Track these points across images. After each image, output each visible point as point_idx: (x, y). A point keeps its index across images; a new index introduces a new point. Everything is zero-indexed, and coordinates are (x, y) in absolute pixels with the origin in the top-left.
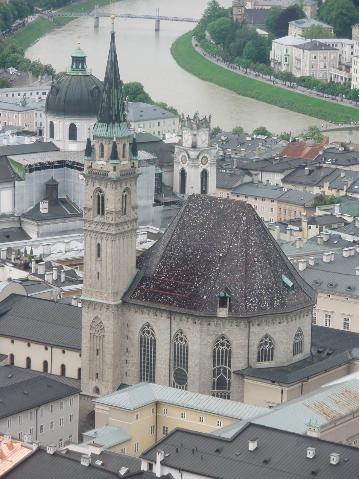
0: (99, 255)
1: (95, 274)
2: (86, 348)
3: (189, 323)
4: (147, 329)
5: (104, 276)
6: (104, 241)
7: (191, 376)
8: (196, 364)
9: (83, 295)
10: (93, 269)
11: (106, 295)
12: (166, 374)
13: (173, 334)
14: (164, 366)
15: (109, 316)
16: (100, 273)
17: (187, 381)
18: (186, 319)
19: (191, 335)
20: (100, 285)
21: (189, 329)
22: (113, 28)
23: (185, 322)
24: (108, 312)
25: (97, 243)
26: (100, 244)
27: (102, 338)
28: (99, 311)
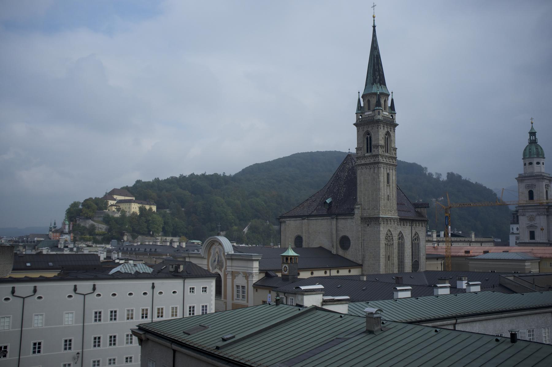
0: (388, 182)
1: (386, 197)
2: (383, 257)
3: (420, 227)
4: (401, 237)
5: (391, 197)
6: (391, 171)
9: (380, 214)
10: (385, 193)
11: (393, 212)
13: (413, 237)
14: (409, 261)
15: (396, 227)
16: (389, 195)
17: (418, 268)
18: (418, 225)
19: (421, 235)
20: (389, 205)
21: (420, 231)
23: (418, 226)
24: (395, 224)
27: (392, 246)
28: (390, 225)
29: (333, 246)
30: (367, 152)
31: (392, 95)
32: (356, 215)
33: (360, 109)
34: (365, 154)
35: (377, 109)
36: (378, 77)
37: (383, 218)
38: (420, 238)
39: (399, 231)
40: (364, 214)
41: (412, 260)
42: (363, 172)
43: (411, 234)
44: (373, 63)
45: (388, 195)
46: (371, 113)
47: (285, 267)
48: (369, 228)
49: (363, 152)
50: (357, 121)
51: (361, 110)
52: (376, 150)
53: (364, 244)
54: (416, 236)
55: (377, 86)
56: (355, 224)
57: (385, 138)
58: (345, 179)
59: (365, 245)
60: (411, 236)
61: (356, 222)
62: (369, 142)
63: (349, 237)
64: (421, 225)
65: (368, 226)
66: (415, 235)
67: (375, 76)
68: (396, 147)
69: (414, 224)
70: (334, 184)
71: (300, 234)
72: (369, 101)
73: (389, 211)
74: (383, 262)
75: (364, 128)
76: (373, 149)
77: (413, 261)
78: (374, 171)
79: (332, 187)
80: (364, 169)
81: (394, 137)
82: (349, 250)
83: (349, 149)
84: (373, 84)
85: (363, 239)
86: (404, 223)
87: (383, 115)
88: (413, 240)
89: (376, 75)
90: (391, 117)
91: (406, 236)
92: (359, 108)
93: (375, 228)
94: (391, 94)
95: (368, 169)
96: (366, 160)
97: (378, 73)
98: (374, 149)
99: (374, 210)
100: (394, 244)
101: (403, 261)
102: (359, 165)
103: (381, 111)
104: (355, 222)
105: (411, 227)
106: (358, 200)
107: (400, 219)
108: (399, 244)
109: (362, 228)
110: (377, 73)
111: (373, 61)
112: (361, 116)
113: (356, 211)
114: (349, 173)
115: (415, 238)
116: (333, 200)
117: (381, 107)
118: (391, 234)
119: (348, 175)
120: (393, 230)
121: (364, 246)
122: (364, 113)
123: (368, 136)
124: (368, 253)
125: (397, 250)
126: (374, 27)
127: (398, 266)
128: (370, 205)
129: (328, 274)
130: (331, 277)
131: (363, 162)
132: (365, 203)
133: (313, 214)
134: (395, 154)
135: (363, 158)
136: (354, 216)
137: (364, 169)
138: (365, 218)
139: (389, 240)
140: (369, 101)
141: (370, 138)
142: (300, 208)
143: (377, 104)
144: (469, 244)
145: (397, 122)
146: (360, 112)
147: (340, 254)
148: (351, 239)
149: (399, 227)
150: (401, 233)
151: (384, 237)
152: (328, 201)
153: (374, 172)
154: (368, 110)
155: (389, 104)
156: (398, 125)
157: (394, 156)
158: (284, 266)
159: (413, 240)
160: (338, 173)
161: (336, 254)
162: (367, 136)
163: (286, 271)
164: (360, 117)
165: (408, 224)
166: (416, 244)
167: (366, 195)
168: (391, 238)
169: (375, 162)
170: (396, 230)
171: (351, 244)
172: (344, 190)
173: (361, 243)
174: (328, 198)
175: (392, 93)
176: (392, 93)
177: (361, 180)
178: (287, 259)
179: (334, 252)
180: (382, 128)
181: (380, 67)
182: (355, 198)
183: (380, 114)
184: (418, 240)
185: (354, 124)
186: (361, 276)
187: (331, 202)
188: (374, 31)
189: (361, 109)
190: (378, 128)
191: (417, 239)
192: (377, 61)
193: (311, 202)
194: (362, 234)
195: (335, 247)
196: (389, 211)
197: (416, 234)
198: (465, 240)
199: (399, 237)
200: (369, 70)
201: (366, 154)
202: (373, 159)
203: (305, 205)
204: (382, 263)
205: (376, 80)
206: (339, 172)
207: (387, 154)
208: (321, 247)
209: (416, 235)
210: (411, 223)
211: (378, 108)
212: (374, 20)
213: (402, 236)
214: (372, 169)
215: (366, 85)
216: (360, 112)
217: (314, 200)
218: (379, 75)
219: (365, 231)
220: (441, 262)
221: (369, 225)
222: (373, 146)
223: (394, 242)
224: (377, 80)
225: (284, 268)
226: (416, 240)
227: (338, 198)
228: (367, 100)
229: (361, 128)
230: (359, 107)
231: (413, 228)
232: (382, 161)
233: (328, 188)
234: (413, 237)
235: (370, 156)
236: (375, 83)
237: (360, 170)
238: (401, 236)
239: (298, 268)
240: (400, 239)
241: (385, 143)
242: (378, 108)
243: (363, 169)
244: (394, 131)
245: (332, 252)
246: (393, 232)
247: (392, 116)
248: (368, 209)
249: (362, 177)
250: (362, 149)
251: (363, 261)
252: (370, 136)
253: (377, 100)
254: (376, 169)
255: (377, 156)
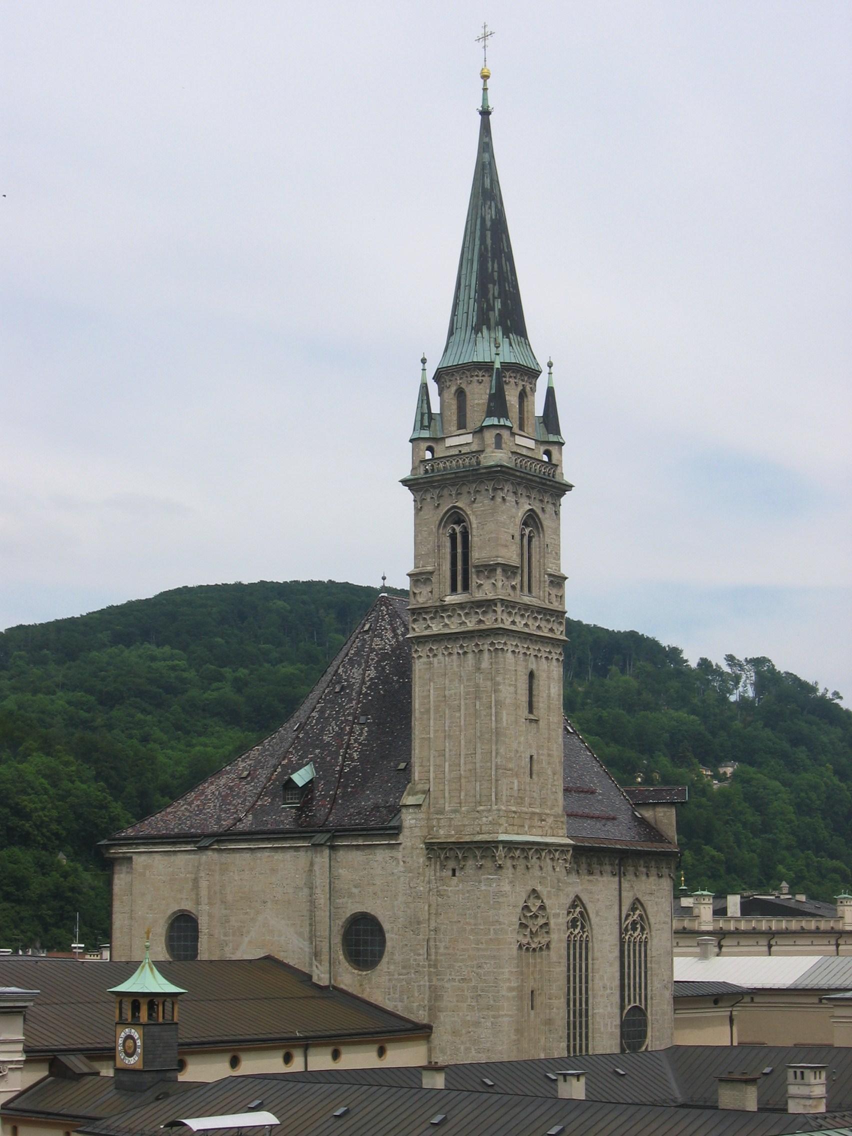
2: (510, 994)
7: (659, 1017)
8: (665, 982)
11: (550, 820)
12: (614, 1030)
13: (624, 916)
14: (609, 1008)
15: (558, 882)
16: (535, 757)
18: (644, 870)
22: (485, 99)
25: (530, 670)
26: (535, 672)
29: (316, 954)
30: (454, 589)
31: (550, 373)
32: (406, 832)
33: (426, 423)
34: (446, 596)
35: (493, 426)
36: (498, 305)
37: (510, 846)
38: (652, 920)
39: (572, 896)
40: (437, 831)
41: (622, 1008)
42: (436, 665)
43: (616, 908)
44: (480, 249)
45: (531, 757)
46: (468, 438)
47: (129, 1037)
48: (457, 886)
49: (436, 590)
50: (414, 469)
51: (429, 427)
52: (487, 585)
53: (436, 947)
54: (638, 912)
55: (493, 335)
56: (402, 869)
57: (522, 536)
58: (366, 694)
59: (442, 950)
60: (617, 913)
61: (407, 860)
62: (459, 550)
63: (381, 919)
64: (654, 871)
65: (454, 875)
66: (633, 909)
67: (488, 301)
68: (564, 571)
69: (631, 869)
70: (322, 712)
71: (187, 906)
72: (461, 394)
73: (536, 818)
74: (511, 1016)
75: (440, 497)
76: (474, 580)
77: (626, 1011)
78: (479, 661)
79: (316, 724)
80: (440, 657)
81: (557, 531)
82: (378, 967)
83: (384, 578)
84: (477, 330)
85: (433, 925)
86: (589, 865)
87: (515, 449)
88: (626, 930)
89: (491, 293)
90: (545, 458)
91: (597, 914)
92: (425, 417)
93: (480, 882)
94: (545, 369)
95: (455, 657)
96: (446, 621)
97: (497, 287)
98: (478, 577)
99: (477, 815)
100: (552, 946)
101: (587, 1010)
102: (421, 640)
103: (505, 434)
104: (404, 862)
105: (617, 879)
106: (416, 776)
107: (575, 848)
108: (570, 942)
109: (429, 882)
110: (494, 290)
111: (477, 242)
112: (430, 449)
113: (408, 819)
114: (384, 668)
115: (634, 923)
116: (317, 772)
117: (507, 418)
118: (542, 908)
119: (376, 677)
120: (549, 892)
121: (436, 953)
122: (439, 440)
123: (458, 529)
124: (454, 980)
125: (566, 969)
126: (485, 113)
127: (569, 1029)
128: (463, 794)
129: (297, 1065)
130: (308, 1077)
131: (436, 628)
132: (441, 787)
133: (240, 827)
134: (561, 598)
135: (436, 612)
136: (401, 837)
137: (440, 657)
138: (443, 846)
139: (534, 930)
140: (461, 394)
141: (465, 535)
142: (190, 804)
143: (492, 404)
144: (833, 942)
145: (568, 478)
146: (426, 434)
147: (342, 986)
148: (386, 926)
149: (574, 878)
150: (577, 901)
151: (515, 920)
152: (301, 777)
153: (479, 669)
154: (459, 428)
155: (539, 408)
156: (569, 487)
157: (555, 606)
158: (123, 1035)
159: (626, 930)
160: (340, 671)
161: (327, 987)
162: (454, 530)
163: (130, 1055)
164: (428, 455)
165: (608, 868)
166: (635, 943)
167: (447, 755)
168: (541, 921)
169: (482, 627)
170: (561, 893)
171: (389, 944)
172: (361, 734)
173: (428, 941)
174: (300, 766)
175: (550, 365)
176: (550, 365)
177: (429, 695)
178: (136, 1007)
179: (321, 976)
180: (511, 498)
181: (506, 267)
182: (402, 766)
183: (503, 445)
184: (643, 929)
185: (405, 482)
186: (424, 1073)
187: (311, 781)
188: (486, 129)
189: (430, 423)
190: (493, 498)
191: (641, 926)
192: (492, 244)
193: (233, 780)
194: (429, 906)
195: (325, 957)
196: (536, 818)
197: (637, 904)
198: (818, 928)
199: (571, 917)
200: (463, 277)
201: (450, 599)
202: (474, 619)
203: (209, 791)
204: (506, 1019)
205: (491, 313)
206: (344, 666)
207: (526, 599)
208: (268, 958)
209: (637, 909)
210: (620, 865)
211: (495, 421)
212: (485, 90)
213: (584, 915)
214: (470, 656)
215: (451, 333)
216: (426, 434)
217: (246, 773)
218: (499, 296)
219: (441, 896)
220: (729, 1013)
221: (457, 874)
222: (476, 567)
223: (554, 936)
224: (494, 316)
225: (124, 1046)
226: (634, 929)
227: (338, 768)
228: (453, 389)
229: (428, 497)
230: (422, 415)
231: (625, 885)
232: (507, 625)
233: (301, 728)
234: (624, 916)
235: (461, 606)
236: (484, 328)
237: (424, 660)
238: (581, 913)
239: (180, 1041)
240: (574, 926)
241: (522, 555)
242: (495, 421)
243: (435, 656)
244: (557, 513)
245: (315, 979)
246: (549, 897)
247: (548, 453)
248: (455, 811)
249: (432, 684)
250: (434, 579)
251: (433, 1010)
252: (465, 528)
253: (493, 391)
254: (486, 655)
255: (489, 606)
